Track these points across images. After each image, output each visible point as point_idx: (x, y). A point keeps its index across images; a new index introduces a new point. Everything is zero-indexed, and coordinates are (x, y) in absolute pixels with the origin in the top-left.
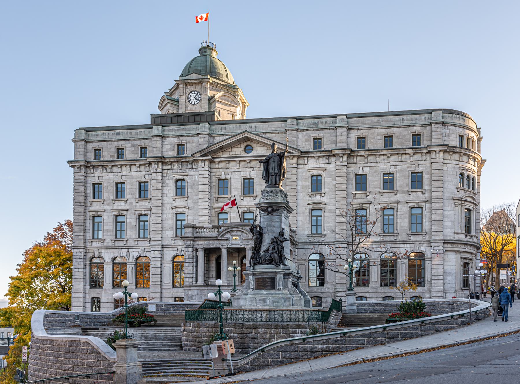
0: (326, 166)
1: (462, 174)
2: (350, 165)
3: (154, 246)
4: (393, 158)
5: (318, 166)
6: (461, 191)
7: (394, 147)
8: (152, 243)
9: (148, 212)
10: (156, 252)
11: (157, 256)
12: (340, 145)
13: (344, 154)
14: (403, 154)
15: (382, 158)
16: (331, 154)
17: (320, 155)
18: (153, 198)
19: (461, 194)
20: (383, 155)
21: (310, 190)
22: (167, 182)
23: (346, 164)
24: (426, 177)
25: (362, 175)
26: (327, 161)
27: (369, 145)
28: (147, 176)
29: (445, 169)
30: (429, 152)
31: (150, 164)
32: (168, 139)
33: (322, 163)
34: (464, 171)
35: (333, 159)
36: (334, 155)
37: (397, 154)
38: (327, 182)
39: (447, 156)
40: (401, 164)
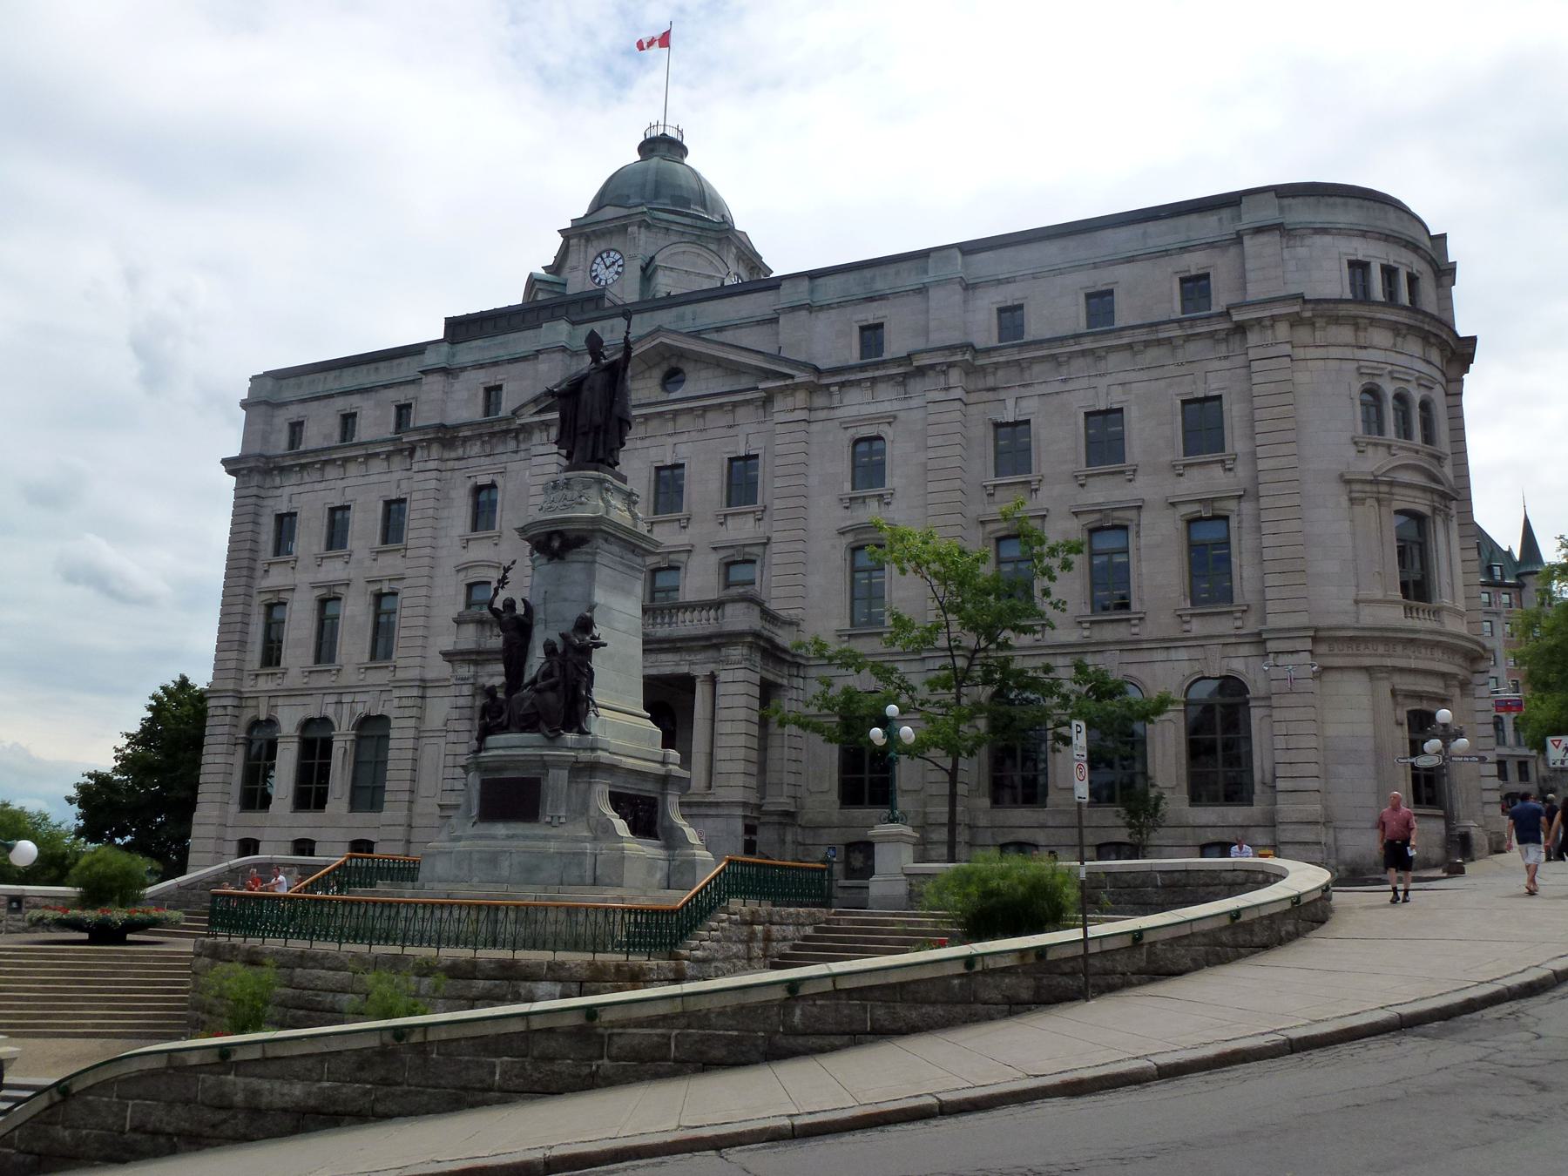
0: (897, 406)
1: (1372, 393)
2: (973, 397)
3: (400, 685)
4: (1114, 360)
5: (872, 409)
6: (1370, 450)
7: (1119, 323)
8: (400, 675)
9: (395, 585)
10: (405, 702)
11: (407, 713)
12: (937, 339)
13: (951, 365)
14: (1147, 344)
15: (1078, 363)
16: (911, 370)
17: (877, 374)
18: (411, 543)
19: (1375, 462)
20: (1083, 353)
21: (848, 486)
22: (453, 494)
23: (958, 393)
24: (1234, 412)
25: (1016, 424)
26: (902, 390)
27: (1035, 327)
28: (404, 484)
29: (1302, 377)
30: (1241, 329)
31: (412, 451)
32: (464, 376)
33: (886, 400)
34: (1377, 380)
35: (916, 385)
36: (921, 371)
37: (1130, 346)
38: (900, 455)
39: (1303, 334)
40: (1144, 375)
